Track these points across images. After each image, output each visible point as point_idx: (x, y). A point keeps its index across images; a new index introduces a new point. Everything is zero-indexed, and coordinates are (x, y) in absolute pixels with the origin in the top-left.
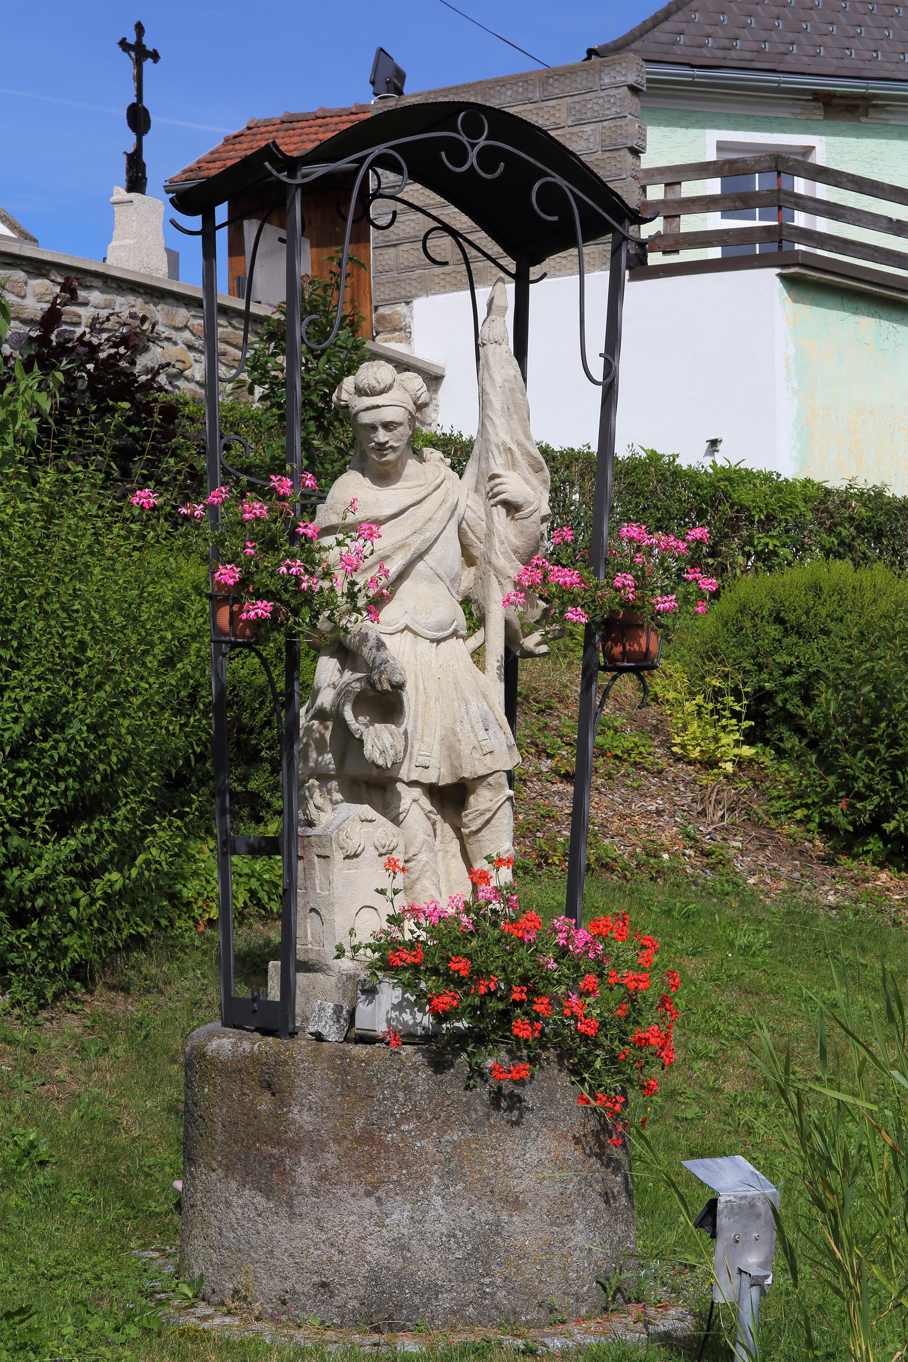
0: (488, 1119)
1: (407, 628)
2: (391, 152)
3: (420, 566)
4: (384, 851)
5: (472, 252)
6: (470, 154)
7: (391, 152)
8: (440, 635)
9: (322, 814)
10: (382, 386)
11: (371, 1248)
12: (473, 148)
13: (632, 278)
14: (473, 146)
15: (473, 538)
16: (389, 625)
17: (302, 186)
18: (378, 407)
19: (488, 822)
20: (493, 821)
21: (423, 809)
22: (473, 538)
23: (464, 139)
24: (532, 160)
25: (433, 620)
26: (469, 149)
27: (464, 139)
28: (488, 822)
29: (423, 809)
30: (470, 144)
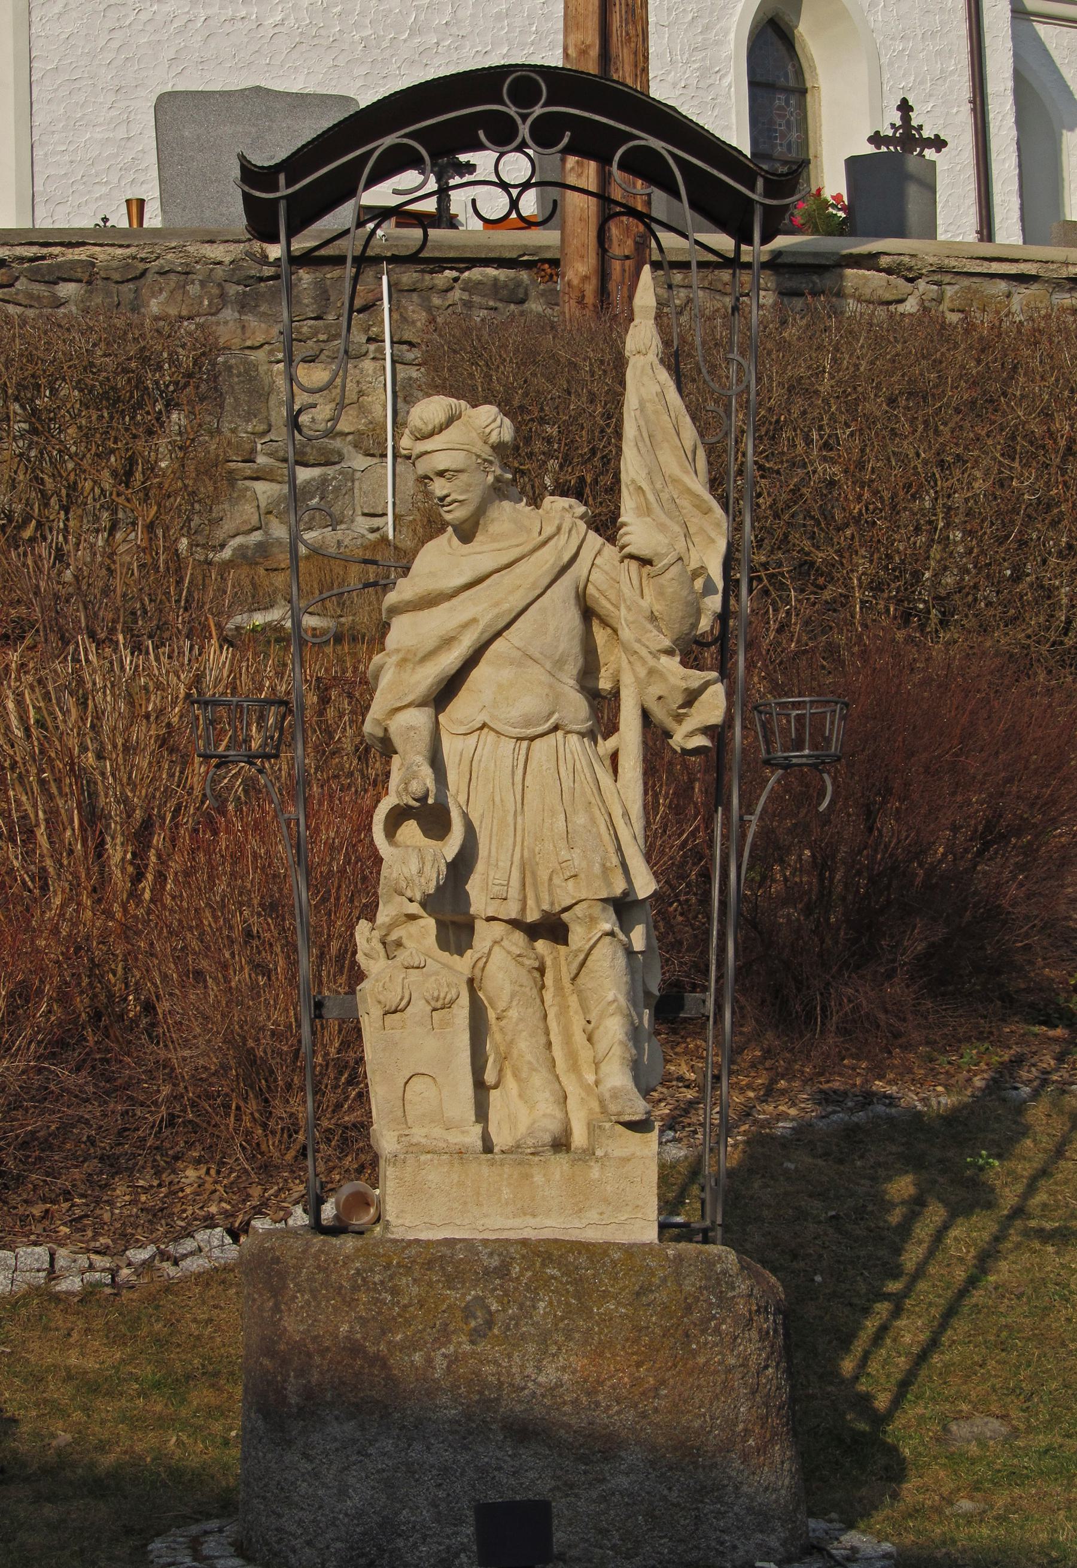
0: (490, 1328)
1: (484, 726)
2: (405, 141)
3: (498, 645)
4: (439, 1005)
5: (654, 226)
6: (521, 127)
7: (405, 141)
8: (531, 731)
9: (372, 962)
10: (430, 427)
11: (354, 1481)
12: (524, 120)
13: (930, 232)
14: (524, 117)
15: (609, 606)
16: (462, 723)
17: (286, 197)
18: (426, 453)
19: (583, 964)
20: (588, 963)
21: (509, 952)
22: (609, 606)
23: (512, 111)
24: (611, 123)
25: (515, 713)
26: (519, 121)
27: (512, 111)
28: (583, 964)
29: (509, 952)
30: (520, 115)
